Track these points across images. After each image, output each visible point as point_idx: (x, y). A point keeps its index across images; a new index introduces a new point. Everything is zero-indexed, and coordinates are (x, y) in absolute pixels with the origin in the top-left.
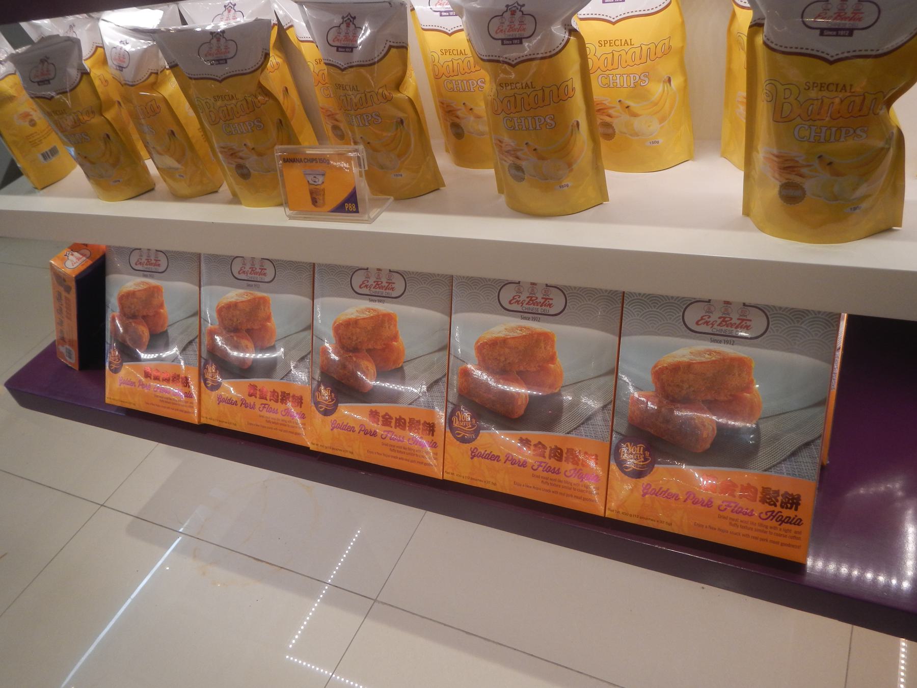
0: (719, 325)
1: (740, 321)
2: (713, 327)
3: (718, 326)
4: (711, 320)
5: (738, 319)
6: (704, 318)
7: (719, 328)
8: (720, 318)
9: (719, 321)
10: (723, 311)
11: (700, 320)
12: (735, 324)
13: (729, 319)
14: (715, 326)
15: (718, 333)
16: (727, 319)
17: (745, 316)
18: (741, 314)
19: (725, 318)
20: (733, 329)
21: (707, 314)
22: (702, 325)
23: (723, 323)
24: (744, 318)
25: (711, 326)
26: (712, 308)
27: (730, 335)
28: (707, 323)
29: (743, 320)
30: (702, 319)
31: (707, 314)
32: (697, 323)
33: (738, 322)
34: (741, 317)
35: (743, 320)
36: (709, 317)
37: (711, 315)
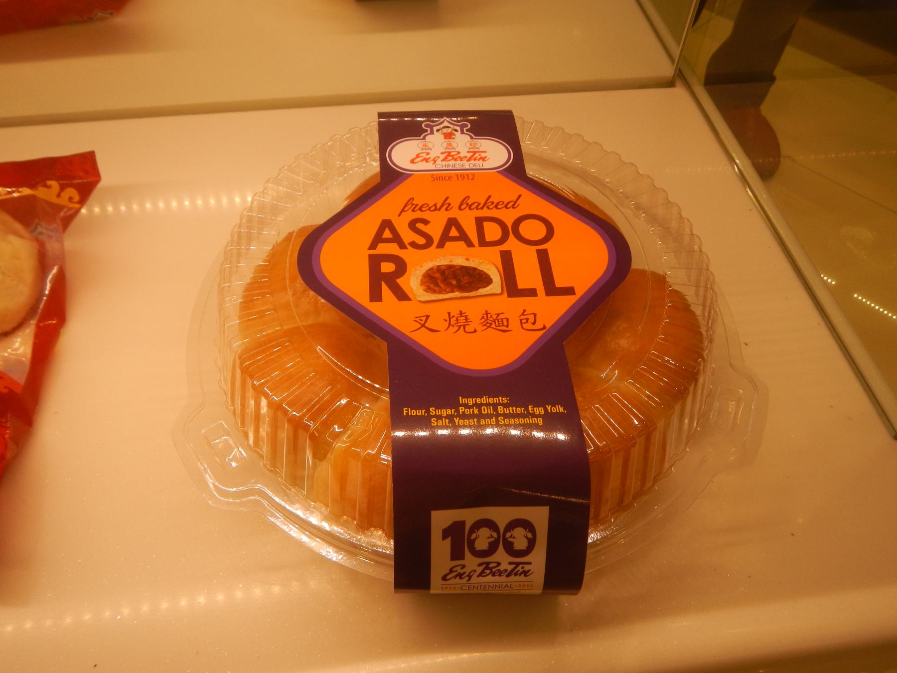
0: (444, 160)
1: (470, 155)
2: (437, 163)
3: (442, 161)
4: (432, 156)
5: (468, 152)
6: (420, 155)
7: (444, 163)
8: (443, 153)
9: (443, 156)
10: (445, 145)
11: (415, 158)
12: (466, 157)
13: (455, 153)
14: (439, 161)
15: (444, 168)
16: (452, 154)
17: (476, 148)
18: (472, 147)
19: (449, 153)
20: (465, 162)
21: (424, 151)
22: (420, 163)
23: (449, 157)
24: (476, 150)
25: (432, 162)
26: (430, 145)
27: (462, 168)
28: (426, 160)
29: (475, 153)
30: (418, 156)
31: (424, 151)
32: (412, 161)
33: (469, 155)
34: (472, 150)
35: (475, 153)
36: (428, 154)
37: (428, 151)
